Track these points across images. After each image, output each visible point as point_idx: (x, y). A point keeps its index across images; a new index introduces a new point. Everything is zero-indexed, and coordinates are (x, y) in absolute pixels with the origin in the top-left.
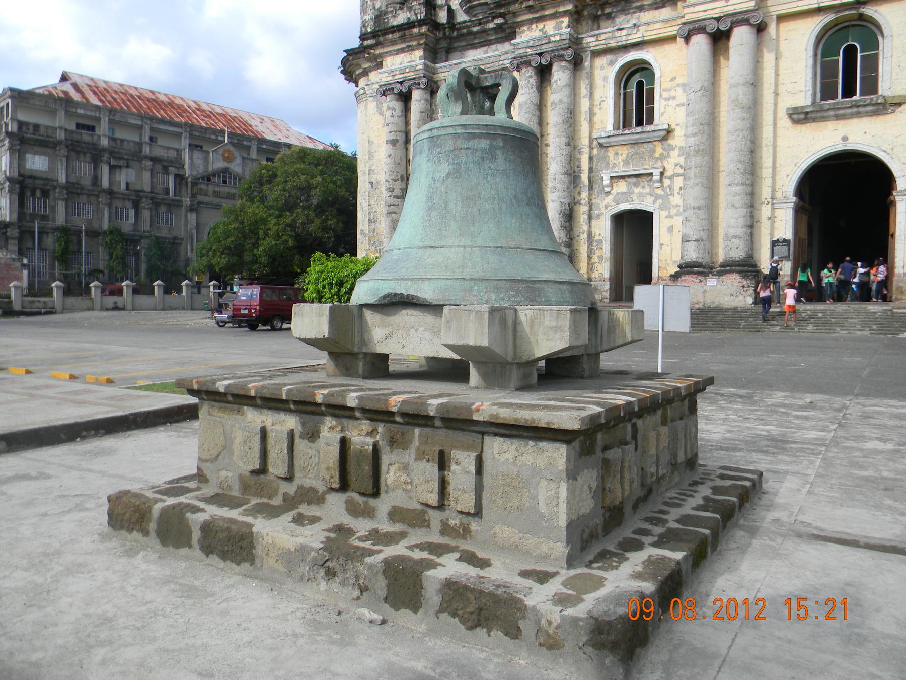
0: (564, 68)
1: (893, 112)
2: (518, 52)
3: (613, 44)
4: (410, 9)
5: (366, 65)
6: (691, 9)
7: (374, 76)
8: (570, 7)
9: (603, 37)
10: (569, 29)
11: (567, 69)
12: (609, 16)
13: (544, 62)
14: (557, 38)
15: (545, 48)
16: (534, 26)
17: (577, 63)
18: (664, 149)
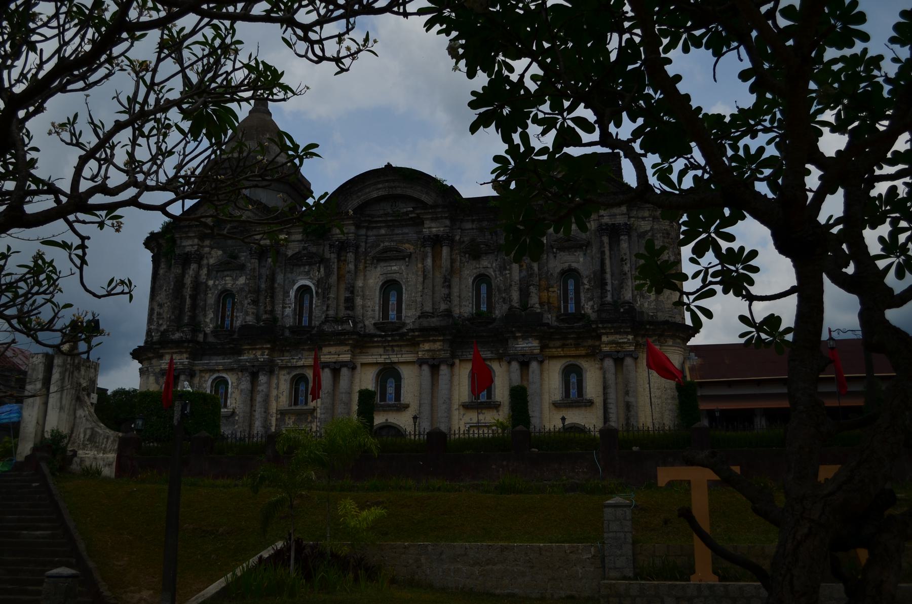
0: (265, 375)
1: (404, 410)
2: (241, 363)
3: (289, 365)
4: (183, 332)
5: (151, 355)
6: (324, 357)
7: (154, 362)
8: (269, 346)
9: (285, 361)
10: (267, 357)
11: (266, 374)
12: (288, 351)
13: (254, 370)
14: (262, 360)
15: (256, 364)
16: (250, 352)
17: (271, 372)
18: (312, 418)
